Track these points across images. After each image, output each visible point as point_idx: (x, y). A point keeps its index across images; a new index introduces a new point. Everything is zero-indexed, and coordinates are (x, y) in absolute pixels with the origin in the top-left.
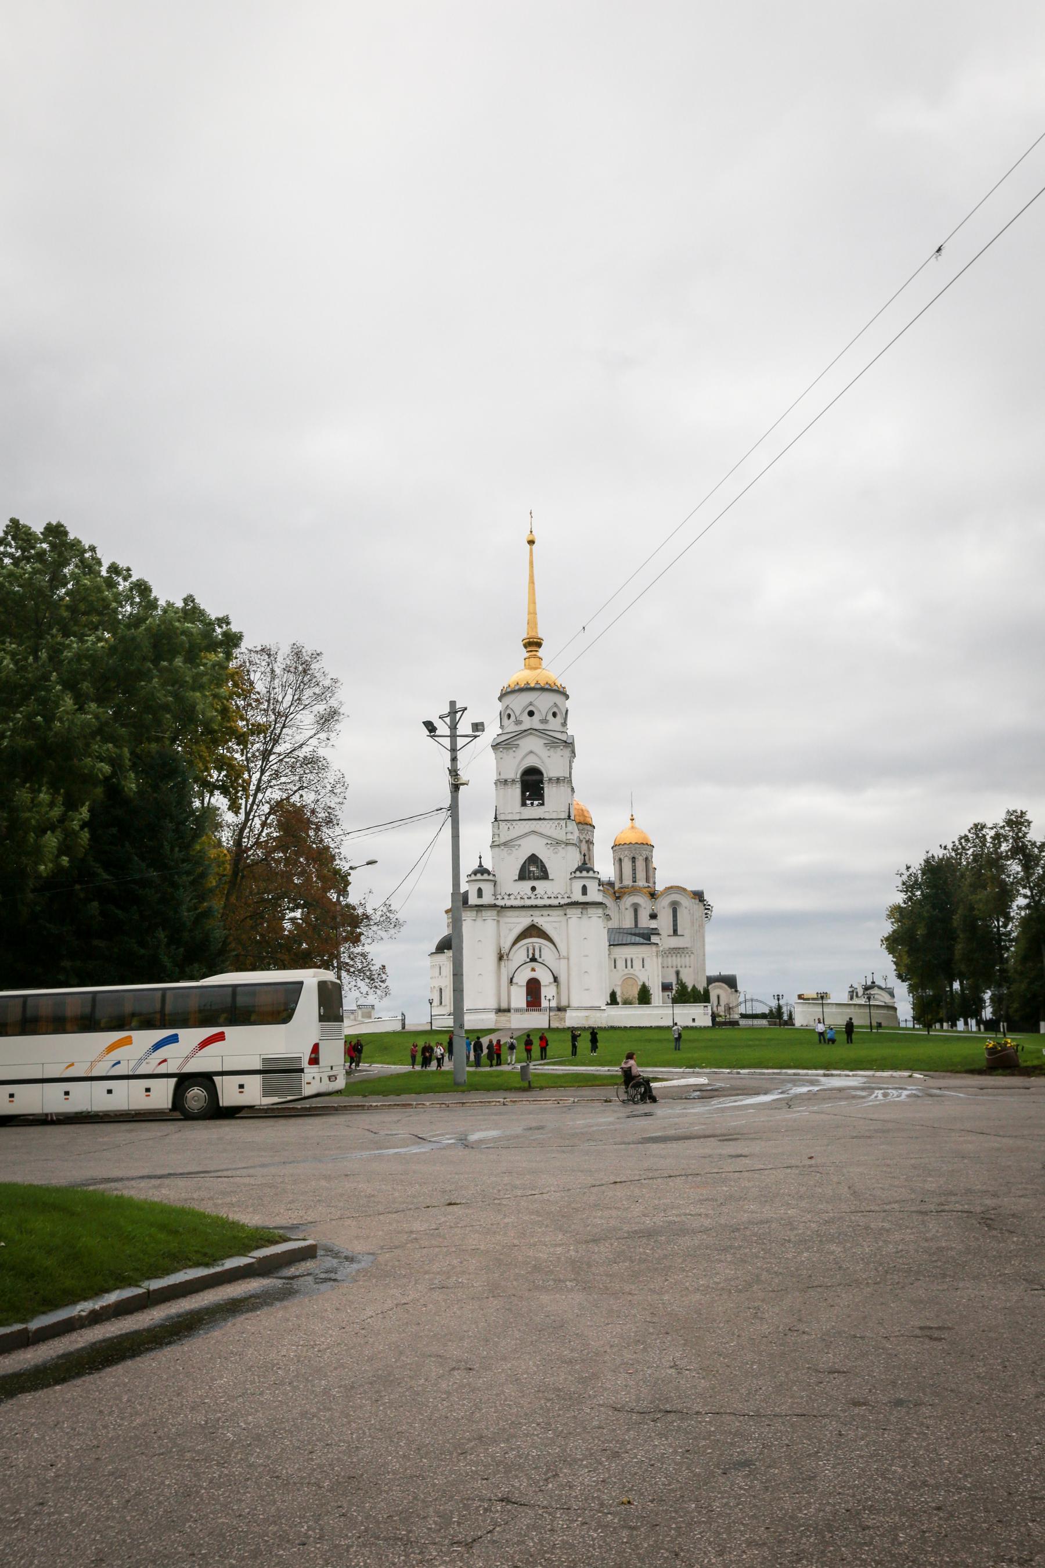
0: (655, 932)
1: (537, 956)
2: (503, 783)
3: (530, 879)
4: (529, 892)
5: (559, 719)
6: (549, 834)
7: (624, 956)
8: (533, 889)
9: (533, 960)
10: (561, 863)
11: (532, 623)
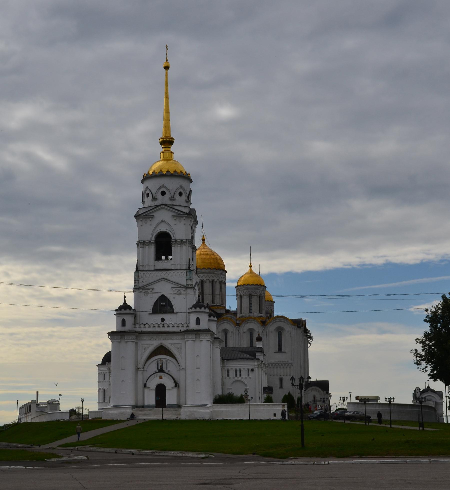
0: (261, 350)
2: (141, 244)
4: (160, 322)
5: (184, 197)
6: (174, 280)
7: (234, 368)
8: (163, 320)
9: (161, 371)
10: (182, 302)
11: (167, 127)
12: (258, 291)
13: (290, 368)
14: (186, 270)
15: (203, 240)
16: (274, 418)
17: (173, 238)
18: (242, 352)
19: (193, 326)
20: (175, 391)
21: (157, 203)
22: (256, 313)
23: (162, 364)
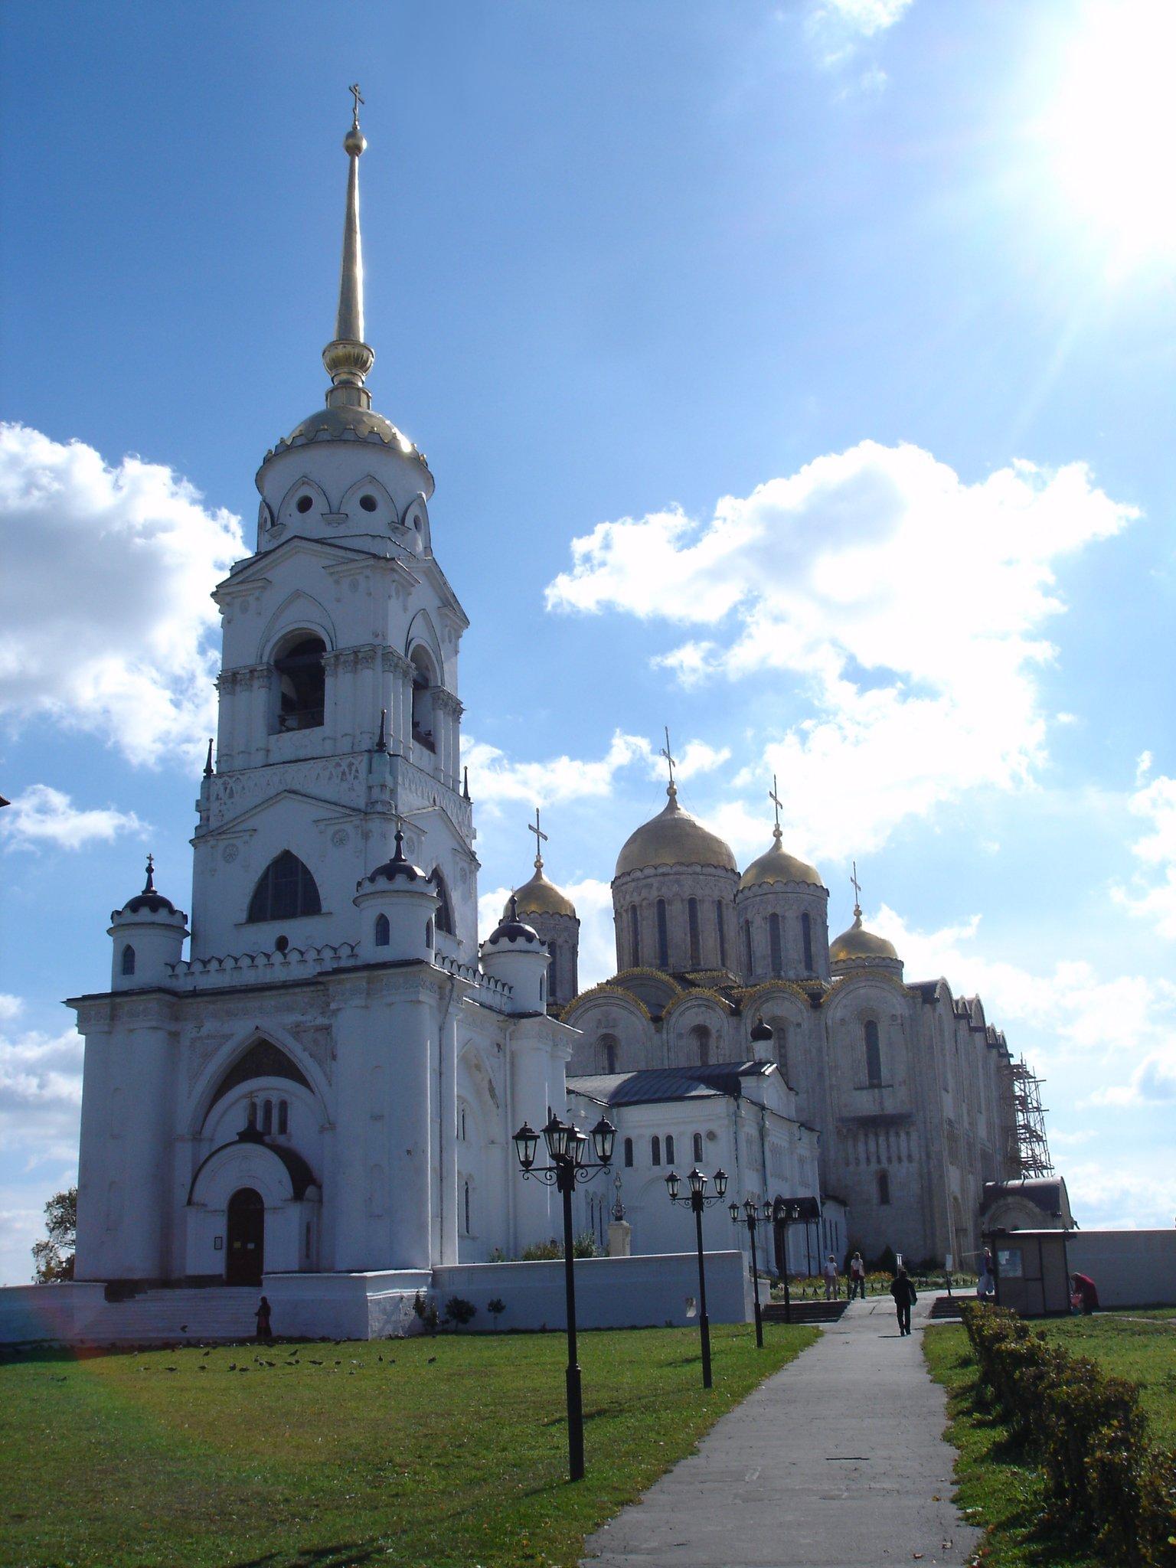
1: (259, 1126)
2: (229, 682)
7: (648, 1133)
8: (282, 944)
9: (251, 1135)
13: (908, 1134)
14: (369, 751)
19: (370, 952)
20: (295, 1214)
21: (283, 539)
23: (268, 1105)
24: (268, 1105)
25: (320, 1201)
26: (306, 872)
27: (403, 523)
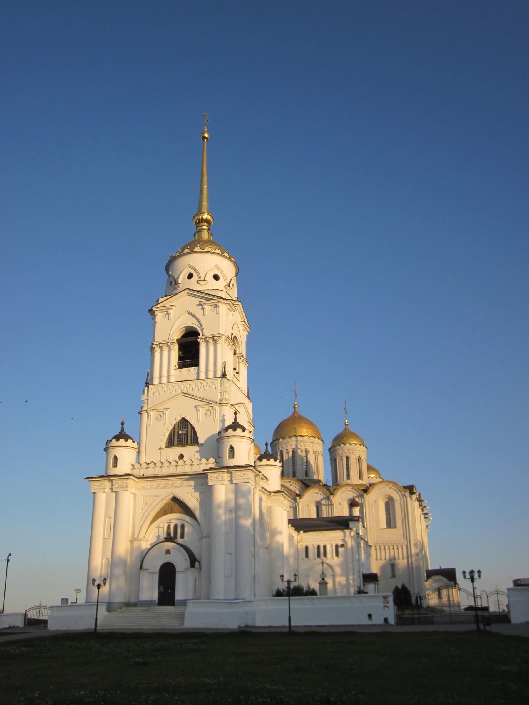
3: (178, 445)
4: (178, 460)
8: (181, 457)
12: (357, 452)
15: (295, 408)
16: (369, 622)
17: (201, 334)
18: (328, 521)
20: (192, 574)
22: (355, 480)
24: (176, 526)
25: (200, 568)
26: (192, 427)
27: (229, 286)
